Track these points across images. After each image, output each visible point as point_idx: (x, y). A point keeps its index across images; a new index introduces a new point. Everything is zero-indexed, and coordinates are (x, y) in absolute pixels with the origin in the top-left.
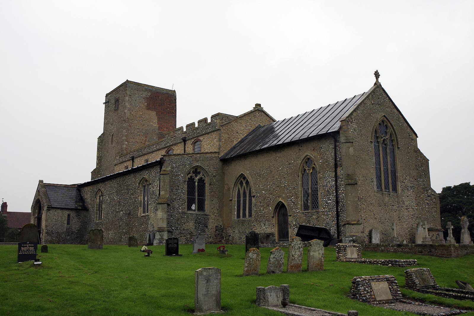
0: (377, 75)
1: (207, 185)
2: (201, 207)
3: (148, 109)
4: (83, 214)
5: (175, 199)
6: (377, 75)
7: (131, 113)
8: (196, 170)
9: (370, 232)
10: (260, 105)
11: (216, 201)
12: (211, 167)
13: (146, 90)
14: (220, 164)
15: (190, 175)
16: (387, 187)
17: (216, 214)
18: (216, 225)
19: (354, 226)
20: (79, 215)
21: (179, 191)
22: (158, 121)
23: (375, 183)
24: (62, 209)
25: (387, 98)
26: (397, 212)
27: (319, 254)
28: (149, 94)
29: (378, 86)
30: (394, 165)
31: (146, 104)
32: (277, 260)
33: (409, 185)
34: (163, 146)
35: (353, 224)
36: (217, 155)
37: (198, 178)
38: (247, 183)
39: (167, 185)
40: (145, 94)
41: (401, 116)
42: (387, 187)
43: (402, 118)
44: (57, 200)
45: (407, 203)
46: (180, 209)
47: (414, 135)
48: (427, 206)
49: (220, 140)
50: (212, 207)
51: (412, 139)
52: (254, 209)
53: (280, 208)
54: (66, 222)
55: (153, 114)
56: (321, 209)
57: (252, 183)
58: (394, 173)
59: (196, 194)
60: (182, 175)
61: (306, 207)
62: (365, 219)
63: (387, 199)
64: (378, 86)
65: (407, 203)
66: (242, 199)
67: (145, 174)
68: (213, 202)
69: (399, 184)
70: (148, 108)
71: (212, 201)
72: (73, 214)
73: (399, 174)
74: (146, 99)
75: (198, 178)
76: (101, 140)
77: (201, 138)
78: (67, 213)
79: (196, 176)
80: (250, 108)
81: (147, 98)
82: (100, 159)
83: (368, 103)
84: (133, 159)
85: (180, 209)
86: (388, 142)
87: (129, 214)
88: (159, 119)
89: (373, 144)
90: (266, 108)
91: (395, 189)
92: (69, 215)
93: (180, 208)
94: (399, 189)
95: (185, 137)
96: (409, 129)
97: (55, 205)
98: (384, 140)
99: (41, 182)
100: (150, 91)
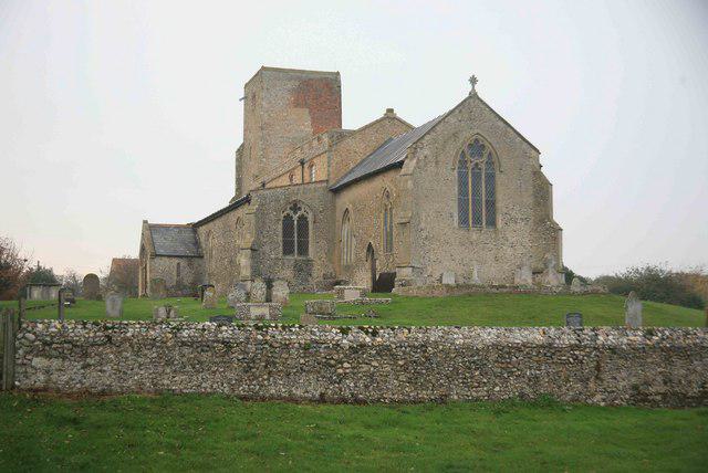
0: (473, 81)
1: (311, 227)
2: (303, 250)
4: (197, 262)
6: (473, 81)
8: (295, 205)
9: (442, 275)
10: (390, 111)
11: (323, 243)
12: (313, 201)
14: (330, 194)
16: (477, 221)
22: (313, 122)
23: (456, 218)
24: (169, 256)
29: (473, 96)
30: (492, 193)
36: (324, 184)
42: (477, 221)
44: (163, 245)
47: (529, 150)
54: (175, 273)
55: (305, 113)
58: (491, 204)
59: (296, 235)
63: (474, 237)
64: (473, 96)
69: (499, 218)
70: (297, 105)
72: (183, 263)
73: (499, 205)
76: (240, 152)
78: (176, 261)
79: (295, 213)
80: (380, 114)
82: (239, 181)
86: (483, 166)
88: (314, 120)
90: (399, 114)
91: (492, 222)
94: (500, 224)
97: (162, 252)
98: (477, 164)
99: (145, 222)
100: (299, 78)
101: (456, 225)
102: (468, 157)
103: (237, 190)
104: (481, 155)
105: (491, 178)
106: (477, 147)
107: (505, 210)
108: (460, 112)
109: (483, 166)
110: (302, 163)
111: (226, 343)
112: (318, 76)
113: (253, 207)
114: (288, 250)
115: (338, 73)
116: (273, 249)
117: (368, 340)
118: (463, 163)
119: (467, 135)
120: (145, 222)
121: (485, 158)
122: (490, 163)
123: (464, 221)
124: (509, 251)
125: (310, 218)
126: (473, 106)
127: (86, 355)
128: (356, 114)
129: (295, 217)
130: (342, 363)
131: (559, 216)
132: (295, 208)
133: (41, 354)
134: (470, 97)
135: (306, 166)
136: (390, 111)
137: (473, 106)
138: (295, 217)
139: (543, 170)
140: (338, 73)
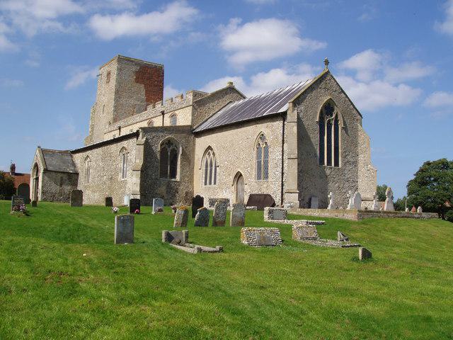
0: (327, 62)
3: (137, 82)
6: (327, 62)
9: (310, 199)
10: (232, 83)
24: (55, 172)
28: (138, 68)
34: (145, 118)
37: (171, 148)
38: (214, 154)
40: (135, 68)
49: (193, 115)
52: (218, 177)
53: (239, 176)
56: (270, 179)
57: (217, 155)
61: (259, 177)
66: (209, 168)
67: (125, 143)
70: (137, 80)
74: (137, 73)
75: (171, 148)
78: (60, 175)
84: (120, 128)
87: (111, 178)
92: (62, 178)
97: (50, 168)
104: (332, 116)
110: (163, 113)
113: (142, 140)
118: (322, 118)
120: (39, 147)
121: (333, 117)
122: (336, 121)
129: (169, 150)
138: (169, 150)
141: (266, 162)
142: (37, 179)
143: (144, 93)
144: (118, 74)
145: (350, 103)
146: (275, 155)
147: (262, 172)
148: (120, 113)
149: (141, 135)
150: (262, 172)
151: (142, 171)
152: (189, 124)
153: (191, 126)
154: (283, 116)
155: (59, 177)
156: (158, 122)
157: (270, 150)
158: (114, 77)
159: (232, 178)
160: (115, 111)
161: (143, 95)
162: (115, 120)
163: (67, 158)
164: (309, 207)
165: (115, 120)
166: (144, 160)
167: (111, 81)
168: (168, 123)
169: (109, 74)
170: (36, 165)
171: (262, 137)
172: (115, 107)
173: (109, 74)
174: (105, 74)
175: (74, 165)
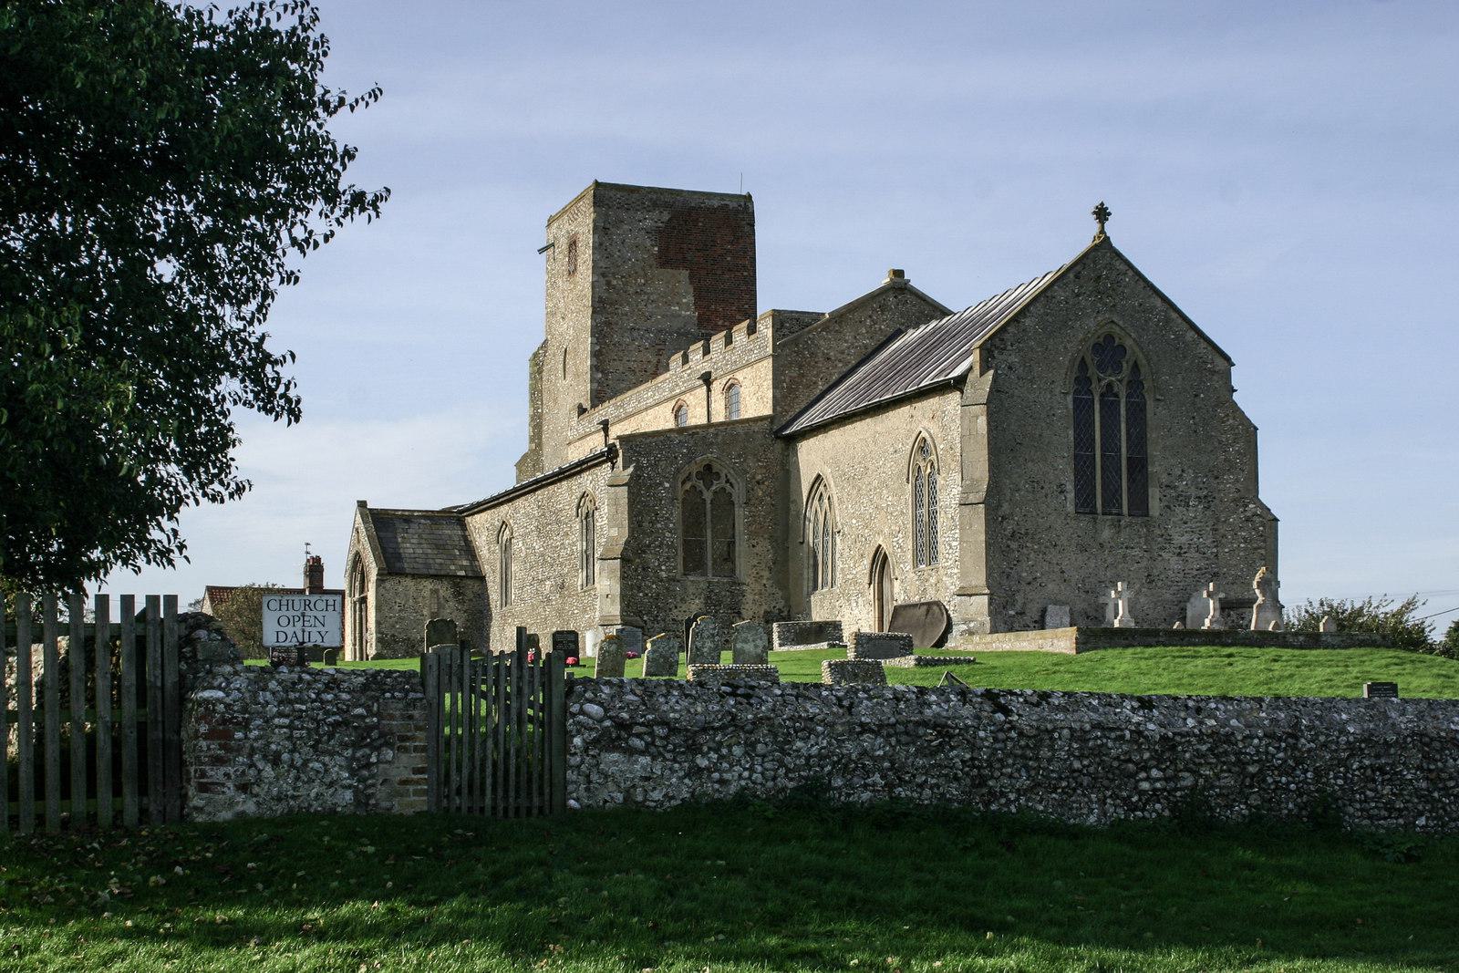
0: (1102, 214)
5: (649, 546)
6: (1102, 214)
7: (608, 283)
8: (708, 467)
9: (1044, 612)
11: (764, 546)
13: (655, 205)
15: (688, 486)
17: (765, 582)
18: (765, 607)
19: (973, 598)
20: (460, 594)
21: (659, 526)
23: (1071, 496)
25: (1130, 273)
26: (1144, 563)
27: (756, 646)
28: (666, 217)
29: (1103, 249)
31: (656, 249)
32: (664, 657)
33: (1193, 492)
35: (970, 595)
39: (622, 513)
41: (1174, 315)
43: (1180, 321)
45: (1179, 540)
46: (662, 570)
47: (1220, 361)
48: (1242, 545)
50: (755, 562)
51: (1213, 372)
58: (1139, 465)
60: (667, 485)
62: (1029, 583)
63: (1106, 534)
64: (1103, 249)
65: (1179, 540)
68: (755, 550)
70: (665, 260)
71: (754, 546)
72: (445, 590)
77: (739, 376)
81: (658, 231)
83: (1061, 295)
84: (605, 426)
85: (662, 570)
86: (1122, 391)
87: (562, 587)
88: (699, 297)
89: (1070, 398)
90: (917, 281)
91: (1140, 506)
93: (663, 568)
94: (1155, 507)
95: (709, 374)
96: (1203, 344)
98: (1110, 385)
100: (667, 206)
101: (1070, 508)
102: (1092, 371)
103: (532, 440)
105: (1138, 413)
106: (1108, 350)
107: (1165, 479)
108: (1077, 277)
109: (1122, 391)
110: (707, 379)
111: (940, 727)
112: (716, 203)
114: (694, 561)
115: (749, 198)
116: (666, 565)
117: (1191, 722)
119: (1090, 325)
120: (362, 504)
122: (1135, 384)
123: (1085, 503)
124: (1175, 563)
125: (738, 493)
126: (1101, 271)
127: (694, 749)
128: (802, 270)
129: (708, 496)
130: (1146, 769)
131: (1270, 492)
132: (708, 472)
133: (613, 745)
134: (1094, 249)
135: (717, 386)
136: (898, 274)
137: (1101, 271)
138: (708, 496)
139: (1235, 396)
140: (749, 198)
141: (933, 515)
142: (363, 600)
143: (689, 299)
144: (598, 248)
145: (1185, 326)
146: (950, 491)
147: (926, 550)
148: (613, 372)
149: (620, 460)
150: (926, 550)
151: (625, 560)
152: (768, 411)
153: (770, 419)
154: (959, 383)
155: (427, 593)
156: (696, 417)
157: (940, 481)
158: (586, 255)
159: (867, 562)
160: (595, 368)
161: (685, 308)
162: (598, 398)
163: (451, 532)
164: (1043, 628)
165: (598, 398)
166: (632, 530)
167: (581, 268)
168: (719, 416)
169: (573, 244)
170: (357, 560)
171: (922, 447)
172: (595, 354)
173: (573, 244)
174: (563, 243)
175: (469, 550)
